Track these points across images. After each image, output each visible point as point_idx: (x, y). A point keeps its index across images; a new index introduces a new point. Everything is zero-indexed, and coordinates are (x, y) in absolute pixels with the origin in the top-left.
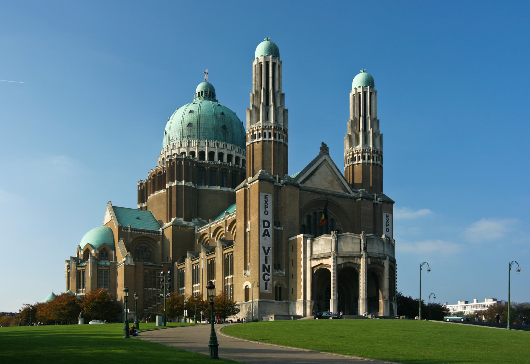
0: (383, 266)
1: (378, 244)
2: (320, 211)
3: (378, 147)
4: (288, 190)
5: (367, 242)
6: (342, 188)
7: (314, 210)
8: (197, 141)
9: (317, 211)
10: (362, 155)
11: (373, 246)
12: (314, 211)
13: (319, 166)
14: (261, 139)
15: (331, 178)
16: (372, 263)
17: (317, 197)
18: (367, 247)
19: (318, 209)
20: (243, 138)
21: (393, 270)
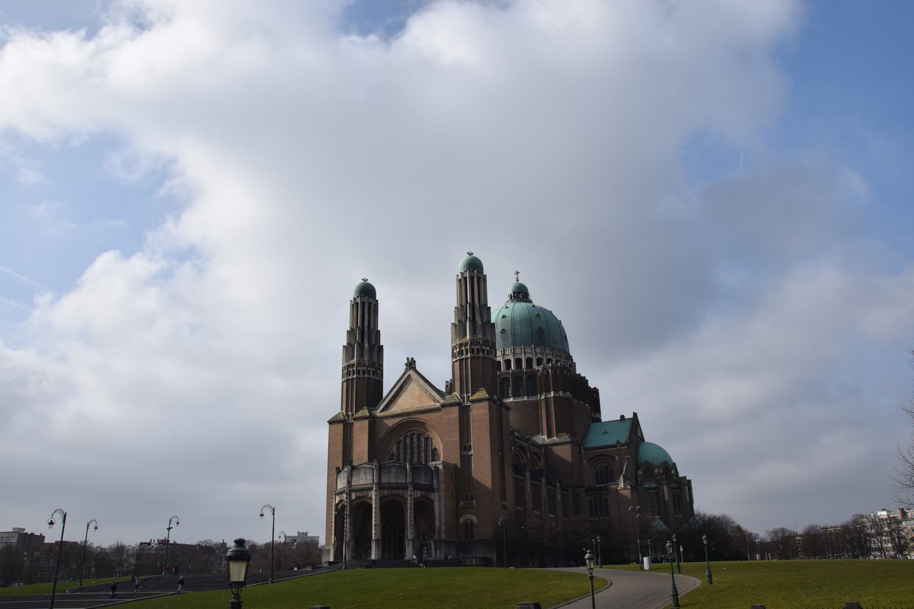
0: (371, 498)
1: (366, 473)
2: (412, 432)
3: (375, 360)
4: (357, 424)
5: (353, 473)
6: (433, 399)
7: (404, 434)
8: (512, 348)
9: (408, 434)
10: (460, 349)
11: (359, 477)
12: (404, 435)
13: (402, 384)
14: (355, 376)
15: (419, 393)
16: (357, 498)
17: (397, 420)
18: (353, 479)
19: (408, 432)
20: (532, 333)
21: (405, 498)
